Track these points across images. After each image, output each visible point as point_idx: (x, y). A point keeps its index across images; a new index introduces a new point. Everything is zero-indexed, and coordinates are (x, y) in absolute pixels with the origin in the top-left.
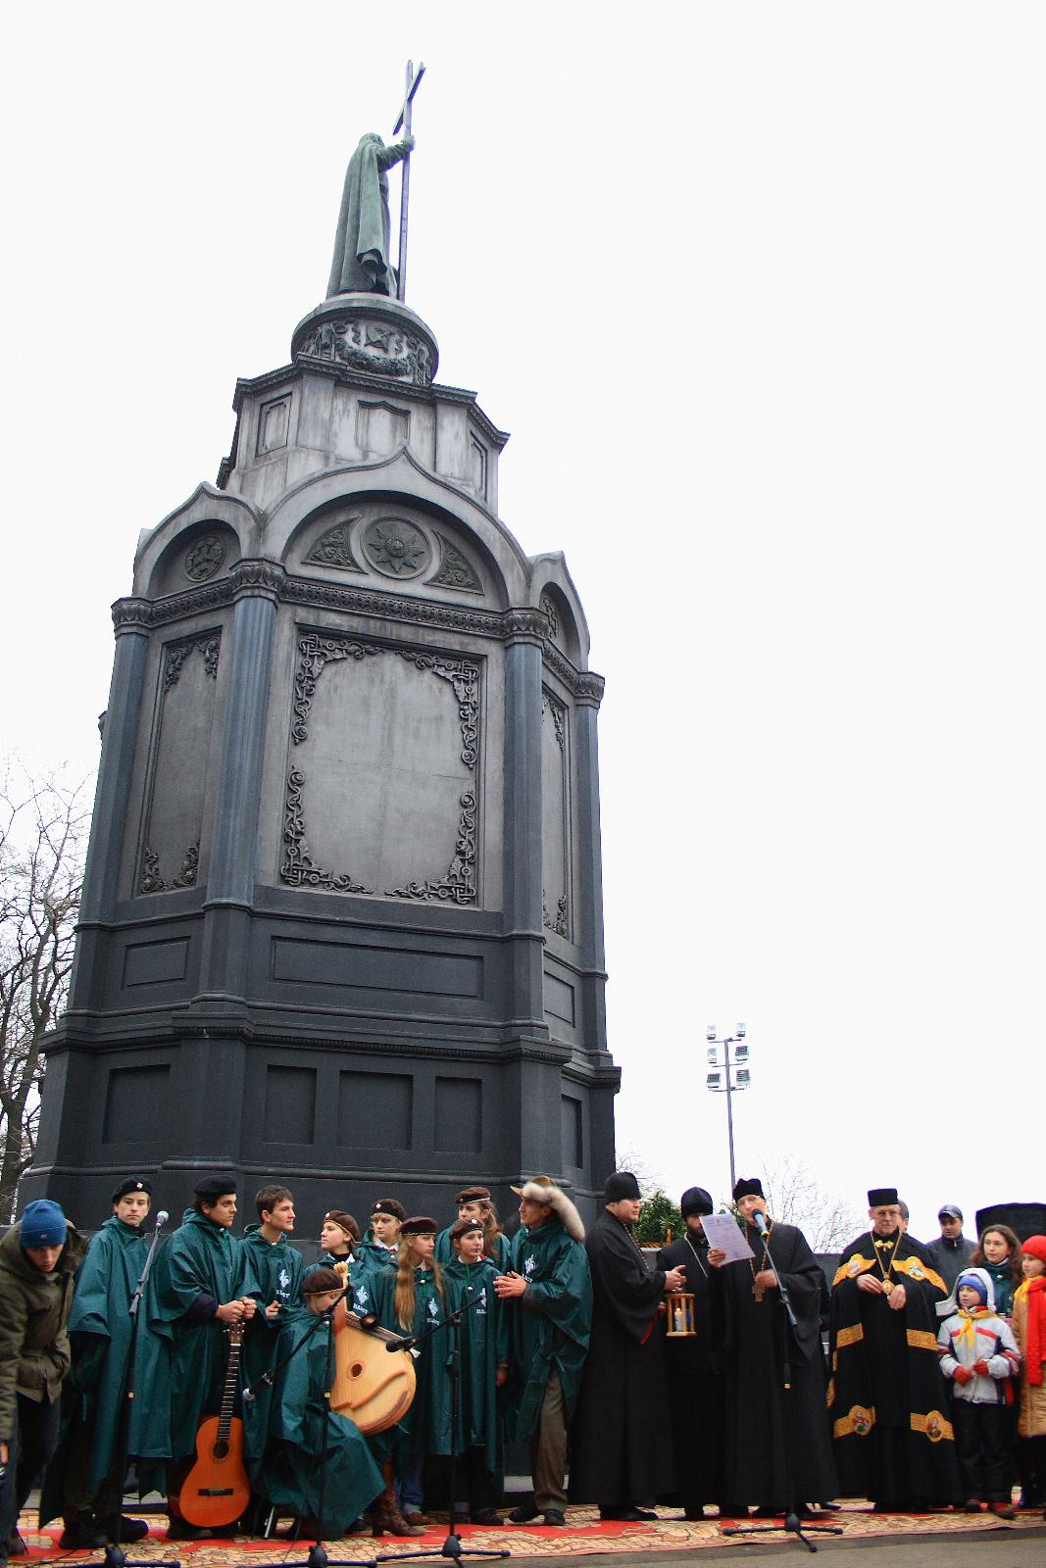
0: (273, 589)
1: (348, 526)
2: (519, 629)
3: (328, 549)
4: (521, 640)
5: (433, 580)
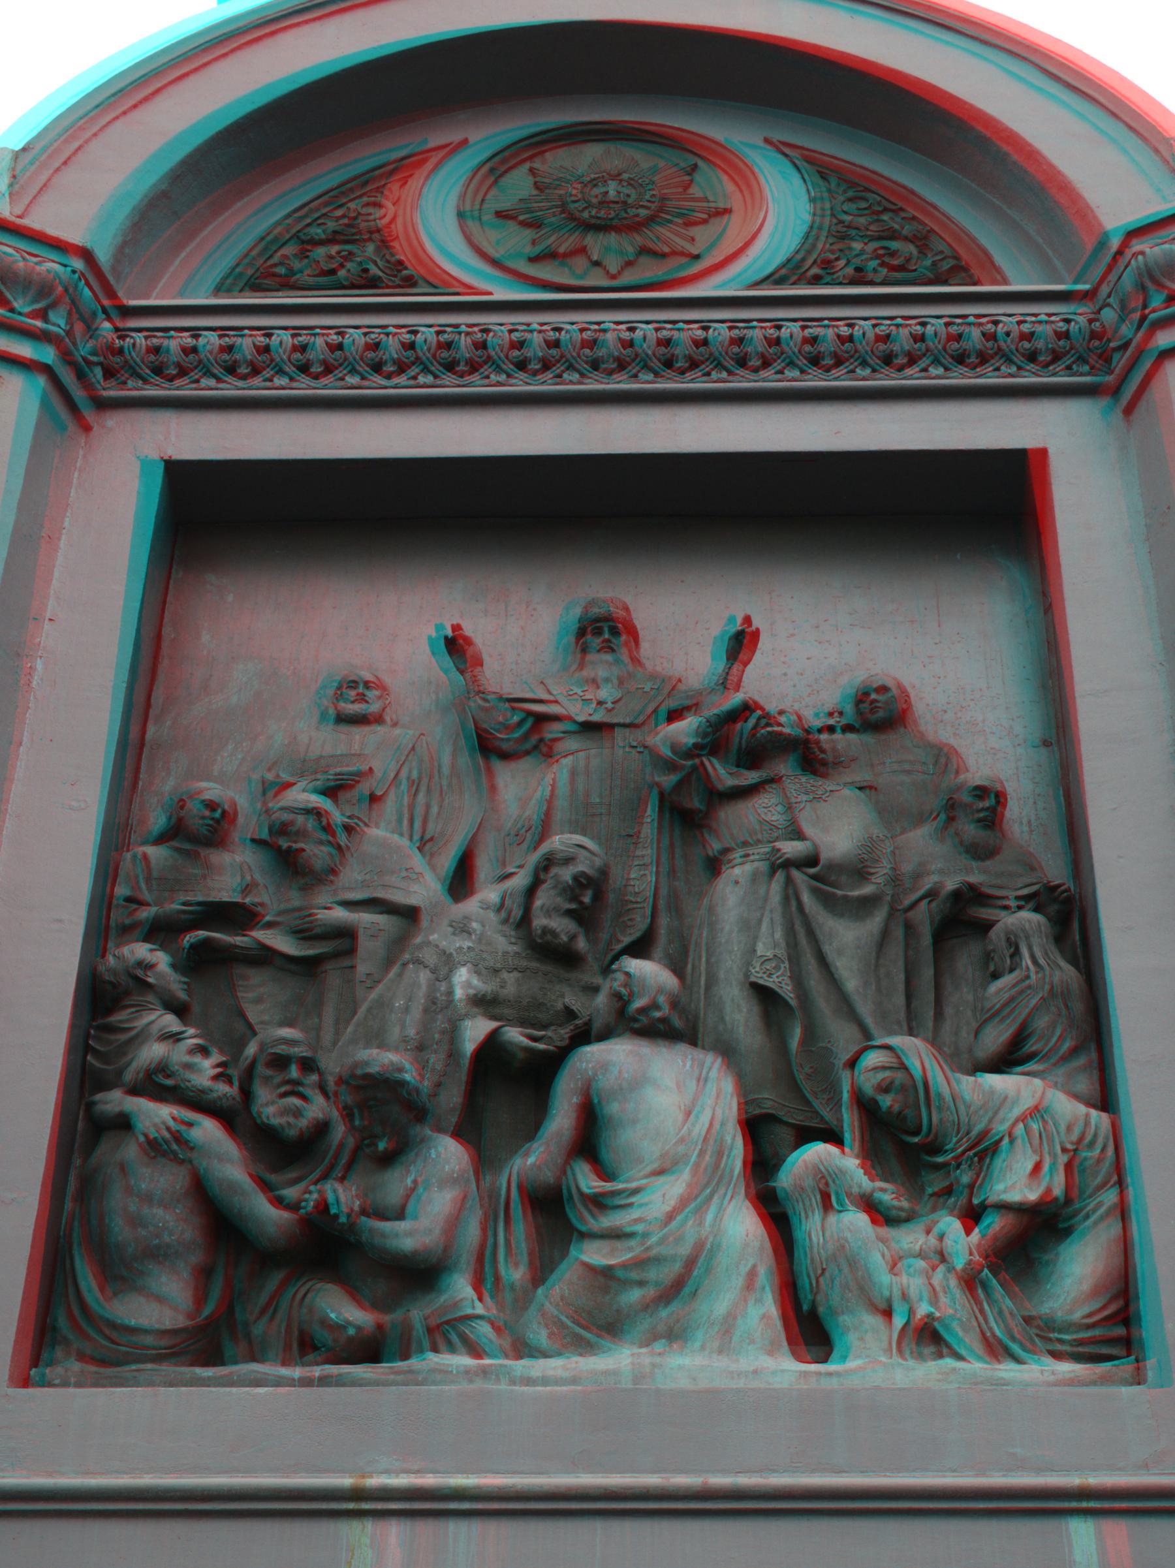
3: (320, 252)
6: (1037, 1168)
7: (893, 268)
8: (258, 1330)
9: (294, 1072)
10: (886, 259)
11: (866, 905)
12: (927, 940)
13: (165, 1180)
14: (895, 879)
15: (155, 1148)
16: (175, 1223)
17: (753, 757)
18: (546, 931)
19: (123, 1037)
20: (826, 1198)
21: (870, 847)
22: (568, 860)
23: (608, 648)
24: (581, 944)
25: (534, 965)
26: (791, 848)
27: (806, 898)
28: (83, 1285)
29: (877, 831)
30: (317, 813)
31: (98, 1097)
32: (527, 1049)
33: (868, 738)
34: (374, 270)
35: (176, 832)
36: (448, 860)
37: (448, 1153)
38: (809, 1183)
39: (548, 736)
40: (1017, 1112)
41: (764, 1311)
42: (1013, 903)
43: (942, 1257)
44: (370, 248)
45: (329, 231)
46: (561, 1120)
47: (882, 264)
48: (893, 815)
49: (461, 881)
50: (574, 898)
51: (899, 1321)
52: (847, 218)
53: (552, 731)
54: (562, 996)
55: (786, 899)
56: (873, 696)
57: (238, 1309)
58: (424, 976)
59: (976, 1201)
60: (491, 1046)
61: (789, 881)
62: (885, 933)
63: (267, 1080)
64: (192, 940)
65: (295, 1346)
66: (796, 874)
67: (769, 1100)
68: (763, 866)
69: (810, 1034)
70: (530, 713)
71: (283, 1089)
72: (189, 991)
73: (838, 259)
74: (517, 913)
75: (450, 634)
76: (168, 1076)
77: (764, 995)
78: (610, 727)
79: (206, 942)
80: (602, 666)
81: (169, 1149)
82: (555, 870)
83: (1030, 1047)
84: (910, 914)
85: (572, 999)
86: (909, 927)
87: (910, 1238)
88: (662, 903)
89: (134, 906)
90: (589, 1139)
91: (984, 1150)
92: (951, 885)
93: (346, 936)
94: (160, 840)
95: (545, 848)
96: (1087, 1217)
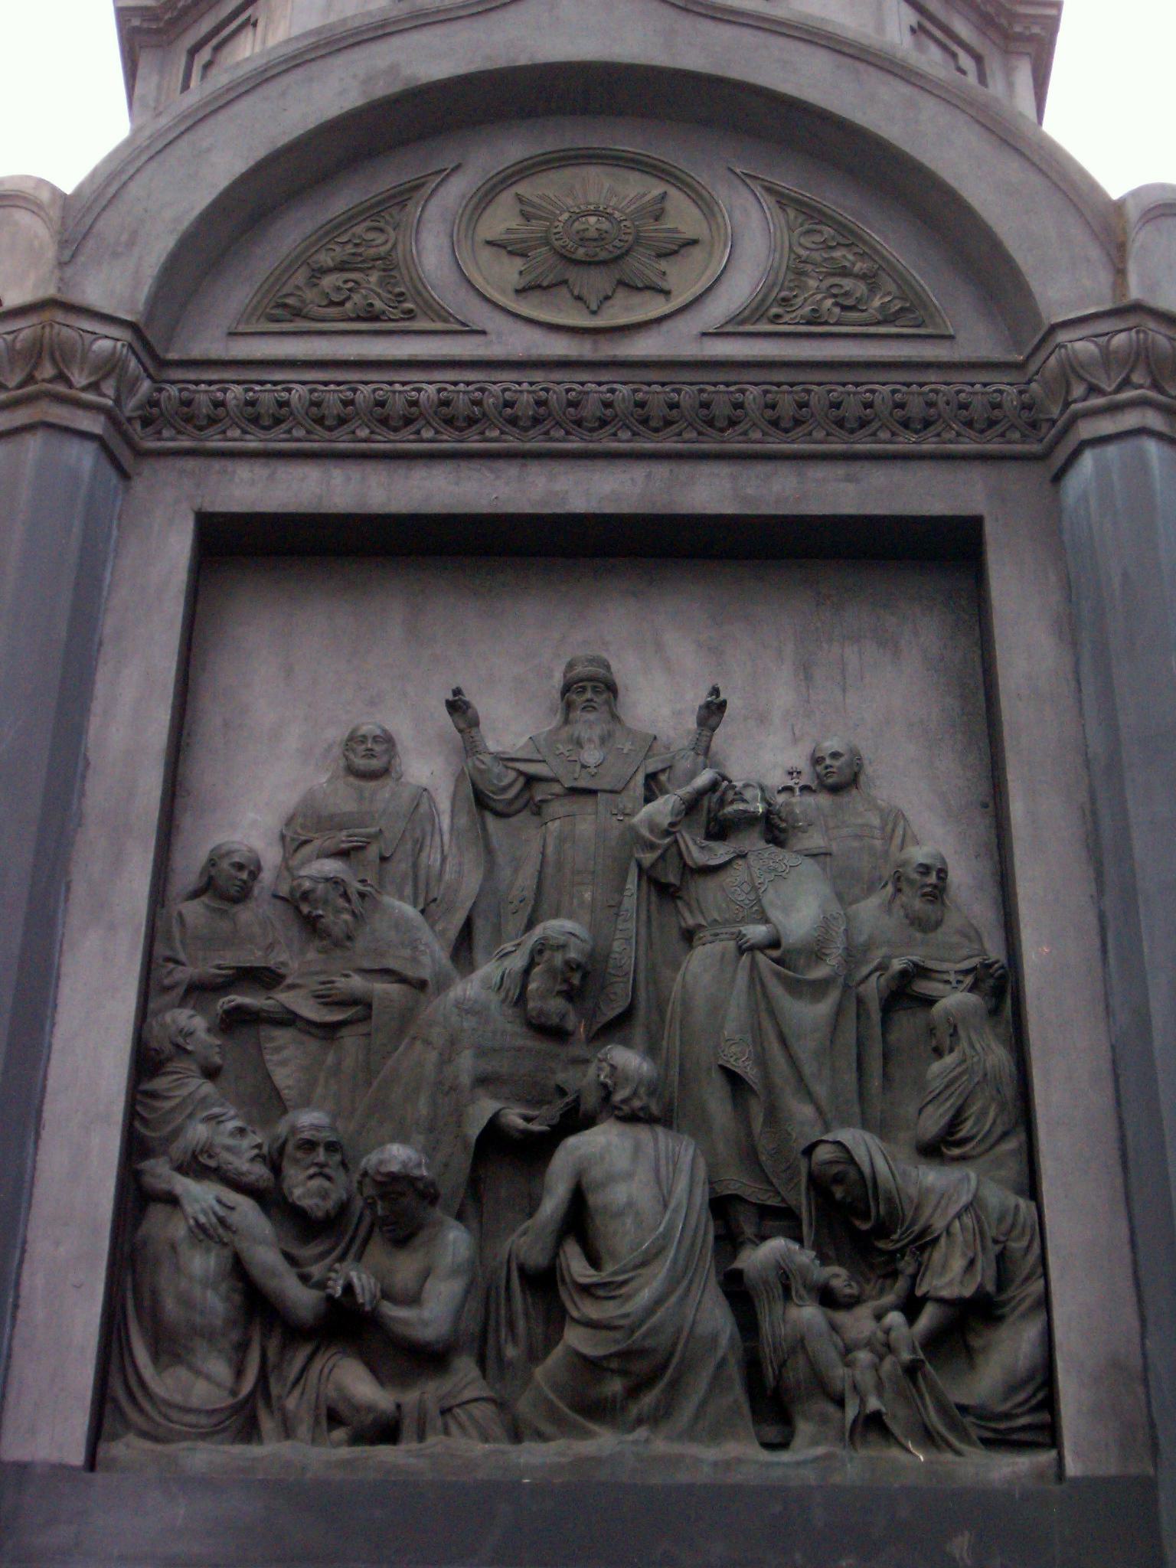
0: (90, 397)
1: (403, 205)
2: (1093, 390)
3: (328, 281)
4: (1106, 426)
5: (737, 319)
6: (972, 1263)
7: (844, 308)
8: (291, 1403)
9: (321, 1155)
10: (840, 300)
12: (876, 1016)
15: (202, 1233)
16: (216, 1304)
17: (720, 830)
18: (541, 1012)
19: (168, 1105)
21: (826, 924)
22: (562, 947)
23: (590, 707)
24: (571, 1022)
25: (530, 1043)
26: (757, 932)
29: (835, 908)
30: (335, 882)
32: (524, 1132)
33: (824, 800)
34: (379, 305)
35: (209, 886)
36: (453, 933)
37: (455, 1241)
38: (772, 1277)
39: (538, 798)
40: (953, 1210)
42: (952, 978)
43: (889, 1348)
44: (374, 277)
45: (338, 259)
46: (553, 1203)
47: (836, 304)
48: (847, 885)
49: (463, 947)
50: (566, 980)
51: (851, 1412)
52: (803, 253)
53: (540, 793)
54: (553, 1072)
55: (752, 980)
56: (828, 762)
57: (272, 1381)
58: (432, 1056)
59: (919, 1293)
60: (494, 1130)
61: (754, 966)
62: (839, 1011)
63: (296, 1161)
64: (226, 1007)
66: (760, 957)
67: (738, 1182)
68: (732, 944)
69: (773, 1114)
70: (521, 773)
71: (312, 1171)
72: (223, 1056)
73: (795, 296)
74: (515, 993)
75: (450, 697)
76: (210, 1156)
77: (733, 1079)
78: (592, 792)
79: (238, 1008)
80: (589, 725)
81: (212, 1232)
82: (547, 954)
83: (965, 1130)
84: (861, 989)
85: (564, 1077)
86: (860, 1001)
87: (859, 1323)
88: (641, 977)
89: (171, 965)
90: (578, 1219)
91: (924, 1242)
92: (897, 965)
93: (362, 1005)
94: (196, 894)
95: (538, 932)
96: (1014, 1309)
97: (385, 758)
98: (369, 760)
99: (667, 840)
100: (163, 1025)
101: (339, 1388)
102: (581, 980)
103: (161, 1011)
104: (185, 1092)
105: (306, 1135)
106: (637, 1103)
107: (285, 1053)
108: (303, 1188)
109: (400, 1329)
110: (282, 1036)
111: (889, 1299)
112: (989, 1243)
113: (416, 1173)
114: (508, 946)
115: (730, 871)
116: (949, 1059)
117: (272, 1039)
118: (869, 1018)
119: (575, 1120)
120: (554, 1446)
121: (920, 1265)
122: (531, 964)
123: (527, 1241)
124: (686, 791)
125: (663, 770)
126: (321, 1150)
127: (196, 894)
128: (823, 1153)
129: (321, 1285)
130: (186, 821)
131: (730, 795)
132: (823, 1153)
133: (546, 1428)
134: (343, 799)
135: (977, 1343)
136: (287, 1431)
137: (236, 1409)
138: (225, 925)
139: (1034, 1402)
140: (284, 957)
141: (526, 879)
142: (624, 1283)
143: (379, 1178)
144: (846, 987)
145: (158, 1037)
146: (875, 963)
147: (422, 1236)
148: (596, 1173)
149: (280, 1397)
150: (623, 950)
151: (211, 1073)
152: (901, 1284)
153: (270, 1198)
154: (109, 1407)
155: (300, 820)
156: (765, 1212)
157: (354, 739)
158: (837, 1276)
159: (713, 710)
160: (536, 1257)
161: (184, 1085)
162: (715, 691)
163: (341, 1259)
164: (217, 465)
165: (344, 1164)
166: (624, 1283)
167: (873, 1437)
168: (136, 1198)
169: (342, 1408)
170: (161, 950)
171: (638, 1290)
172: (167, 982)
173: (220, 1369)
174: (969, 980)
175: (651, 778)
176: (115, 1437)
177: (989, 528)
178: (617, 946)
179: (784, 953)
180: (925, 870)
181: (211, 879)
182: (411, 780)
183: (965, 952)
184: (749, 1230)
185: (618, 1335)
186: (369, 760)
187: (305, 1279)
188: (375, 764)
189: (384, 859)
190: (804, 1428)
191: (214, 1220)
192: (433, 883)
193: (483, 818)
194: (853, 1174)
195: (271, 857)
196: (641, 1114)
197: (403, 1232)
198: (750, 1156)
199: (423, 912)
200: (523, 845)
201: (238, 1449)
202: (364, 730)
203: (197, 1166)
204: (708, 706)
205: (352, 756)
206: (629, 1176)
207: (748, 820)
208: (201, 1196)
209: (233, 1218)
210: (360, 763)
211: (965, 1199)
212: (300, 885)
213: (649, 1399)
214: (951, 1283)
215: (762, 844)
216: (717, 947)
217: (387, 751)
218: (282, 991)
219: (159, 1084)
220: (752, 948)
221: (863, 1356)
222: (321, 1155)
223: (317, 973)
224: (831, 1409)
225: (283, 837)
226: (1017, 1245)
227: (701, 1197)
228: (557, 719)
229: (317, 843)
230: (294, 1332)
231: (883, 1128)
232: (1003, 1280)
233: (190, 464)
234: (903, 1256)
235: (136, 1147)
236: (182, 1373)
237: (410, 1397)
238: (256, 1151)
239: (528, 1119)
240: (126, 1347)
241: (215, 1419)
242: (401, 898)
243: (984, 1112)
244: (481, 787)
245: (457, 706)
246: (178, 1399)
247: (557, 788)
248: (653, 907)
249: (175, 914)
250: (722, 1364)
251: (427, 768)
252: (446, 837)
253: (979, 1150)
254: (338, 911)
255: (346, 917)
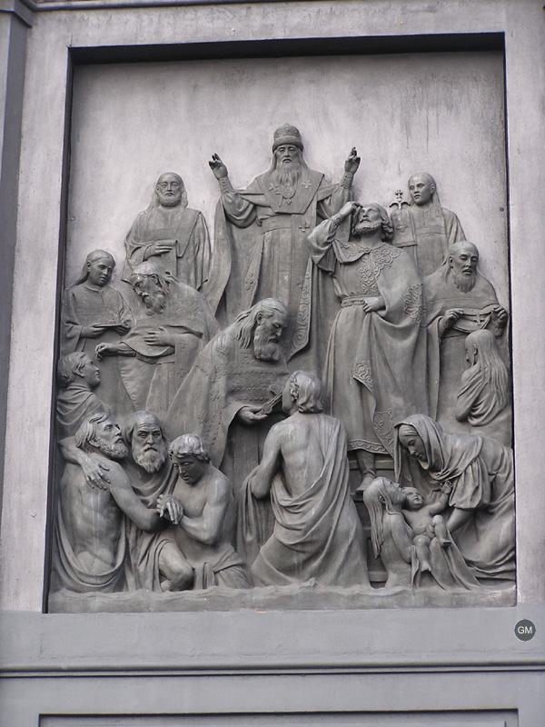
8: (141, 568)
11: (405, 332)
13: (95, 499)
14: (424, 310)
16: (100, 520)
17: (356, 236)
20: (384, 505)
26: (372, 301)
27: (378, 327)
28: (64, 545)
31: (62, 441)
33: (414, 210)
39: (260, 217)
40: (468, 462)
41: (358, 559)
53: (261, 214)
55: (370, 329)
57: (132, 557)
58: (206, 380)
59: (450, 505)
60: (238, 422)
62: (417, 342)
63: (139, 442)
64: (100, 350)
65: (157, 577)
66: (375, 316)
70: (251, 203)
77: (360, 384)
78: (290, 214)
82: (263, 320)
87: (421, 519)
89: (71, 325)
90: (279, 467)
91: (453, 478)
92: (448, 314)
93: (170, 348)
94: (82, 281)
96: (500, 509)
97: (178, 196)
98: (171, 193)
99: (327, 247)
100: (68, 363)
101: (165, 561)
102: (283, 331)
103: (66, 354)
104: (80, 401)
105: (142, 429)
106: (310, 405)
107: (132, 373)
108: (142, 456)
109: (192, 532)
110: (132, 362)
111: (437, 505)
112: (486, 475)
113: (197, 452)
114: (244, 313)
115: (361, 263)
116: (474, 369)
117: (124, 365)
118: (432, 342)
119: (279, 413)
120: (270, 588)
121: (452, 489)
122: (256, 325)
123: (255, 479)
124: (338, 215)
125: (327, 198)
126: (150, 436)
127: (82, 281)
128: (404, 430)
129: (154, 506)
130: (74, 236)
131: (361, 218)
132: (404, 430)
133: (267, 580)
134: (156, 224)
135: (481, 528)
136: (139, 584)
137: (114, 574)
138: (97, 300)
139: (507, 558)
140: (129, 317)
141: (251, 271)
142: (302, 505)
143: (180, 456)
144: (421, 327)
145: (67, 371)
146: (438, 311)
147: (203, 482)
148: (287, 447)
149: (135, 565)
150: (304, 310)
151: (94, 387)
152: (443, 497)
153: (125, 461)
154: (52, 573)
155: (133, 234)
156: (377, 456)
157: (161, 184)
158: (411, 493)
159: (354, 162)
160: (259, 489)
161: (80, 396)
162: (354, 153)
163: (162, 492)
164: (78, 14)
165: (163, 438)
166: (302, 505)
167: (426, 580)
168: (59, 462)
169: (166, 572)
170: (64, 317)
171: (310, 509)
172: (69, 335)
173: (106, 553)
174: (487, 319)
175: (320, 203)
176: (57, 590)
177: (509, 42)
178: (301, 308)
179: (388, 313)
180: (465, 257)
181: (88, 273)
182: (193, 208)
183: (486, 303)
184: (369, 467)
185: (298, 533)
186: (171, 193)
187: (145, 502)
188: (172, 198)
189: (178, 258)
190: (392, 577)
191: (99, 478)
192: (205, 270)
193: (231, 229)
194: (418, 440)
195: (120, 256)
196: (312, 410)
197: (194, 480)
198: (367, 427)
199: (199, 290)
200: (254, 242)
201: (115, 596)
202: (166, 179)
203: (87, 446)
204: (350, 160)
205: (160, 194)
206: (305, 447)
207: (369, 233)
208: (91, 463)
209: (108, 475)
210: (165, 198)
211: (474, 455)
212: (135, 278)
213: (315, 564)
214: (465, 500)
215: (381, 244)
216: (352, 309)
217: (179, 189)
218: (129, 337)
219: (68, 396)
220: (370, 312)
221: (420, 539)
222: (150, 439)
223: (147, 327)
224: (405, 566)
225: (126, 245)
226: (502, 476)
227: (342, 454)
228: (269, 166)
229: (144, 249)
230: (141, 532)
231: (436, 411)
232: (493, 497)
233: (64, 15)
234: (444, 483)
235: (59, 431)
236: (86, 555)
237: (198, 566)
238: (118, 437)
239: (255, 412)
240: (59, 541)
241: (104, 580)
242: (189, 282)
243: (489, 400)
244: (229, 212)
245: (215, 164)
246: (87, 572)
247: (270, 212)
248: (320, 279)
249: (71, 295)
250: (350, 546)
251: (203, 198)
252: (212, 241)
253: (486, 421)
254: (155, 293)
255: (160, 296)
